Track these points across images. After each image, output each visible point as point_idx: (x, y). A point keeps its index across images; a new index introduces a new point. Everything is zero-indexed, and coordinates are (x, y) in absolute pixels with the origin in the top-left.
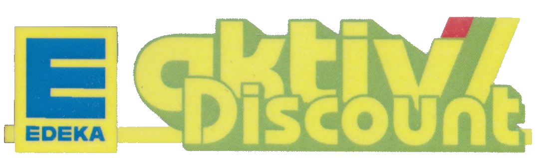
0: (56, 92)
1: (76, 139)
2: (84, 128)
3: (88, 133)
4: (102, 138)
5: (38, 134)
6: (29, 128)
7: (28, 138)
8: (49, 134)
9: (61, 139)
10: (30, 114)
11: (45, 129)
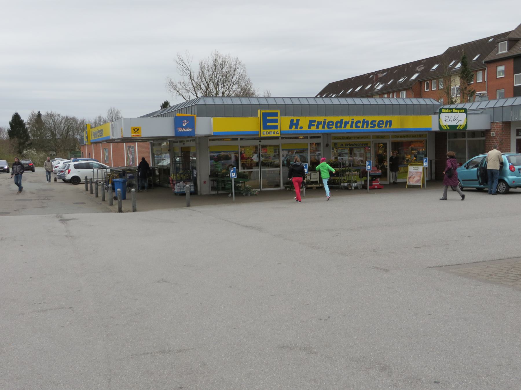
0: (268, 124)
1: (273, 134)
2: (275, 132)
3: (276, 133)
4: (278, 134)
5: (265, 133)
6: (263, 132)
7: (263, 134)
8: (267, 133)
9: (270, 134)
10: (263, 129)
11: (266, 132)
